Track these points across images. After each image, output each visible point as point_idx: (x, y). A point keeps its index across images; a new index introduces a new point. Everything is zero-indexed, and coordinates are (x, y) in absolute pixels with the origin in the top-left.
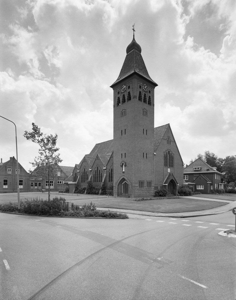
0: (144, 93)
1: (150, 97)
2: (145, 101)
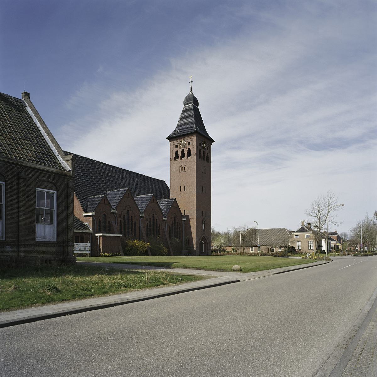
0: (203, 150)
1: (207, 153)
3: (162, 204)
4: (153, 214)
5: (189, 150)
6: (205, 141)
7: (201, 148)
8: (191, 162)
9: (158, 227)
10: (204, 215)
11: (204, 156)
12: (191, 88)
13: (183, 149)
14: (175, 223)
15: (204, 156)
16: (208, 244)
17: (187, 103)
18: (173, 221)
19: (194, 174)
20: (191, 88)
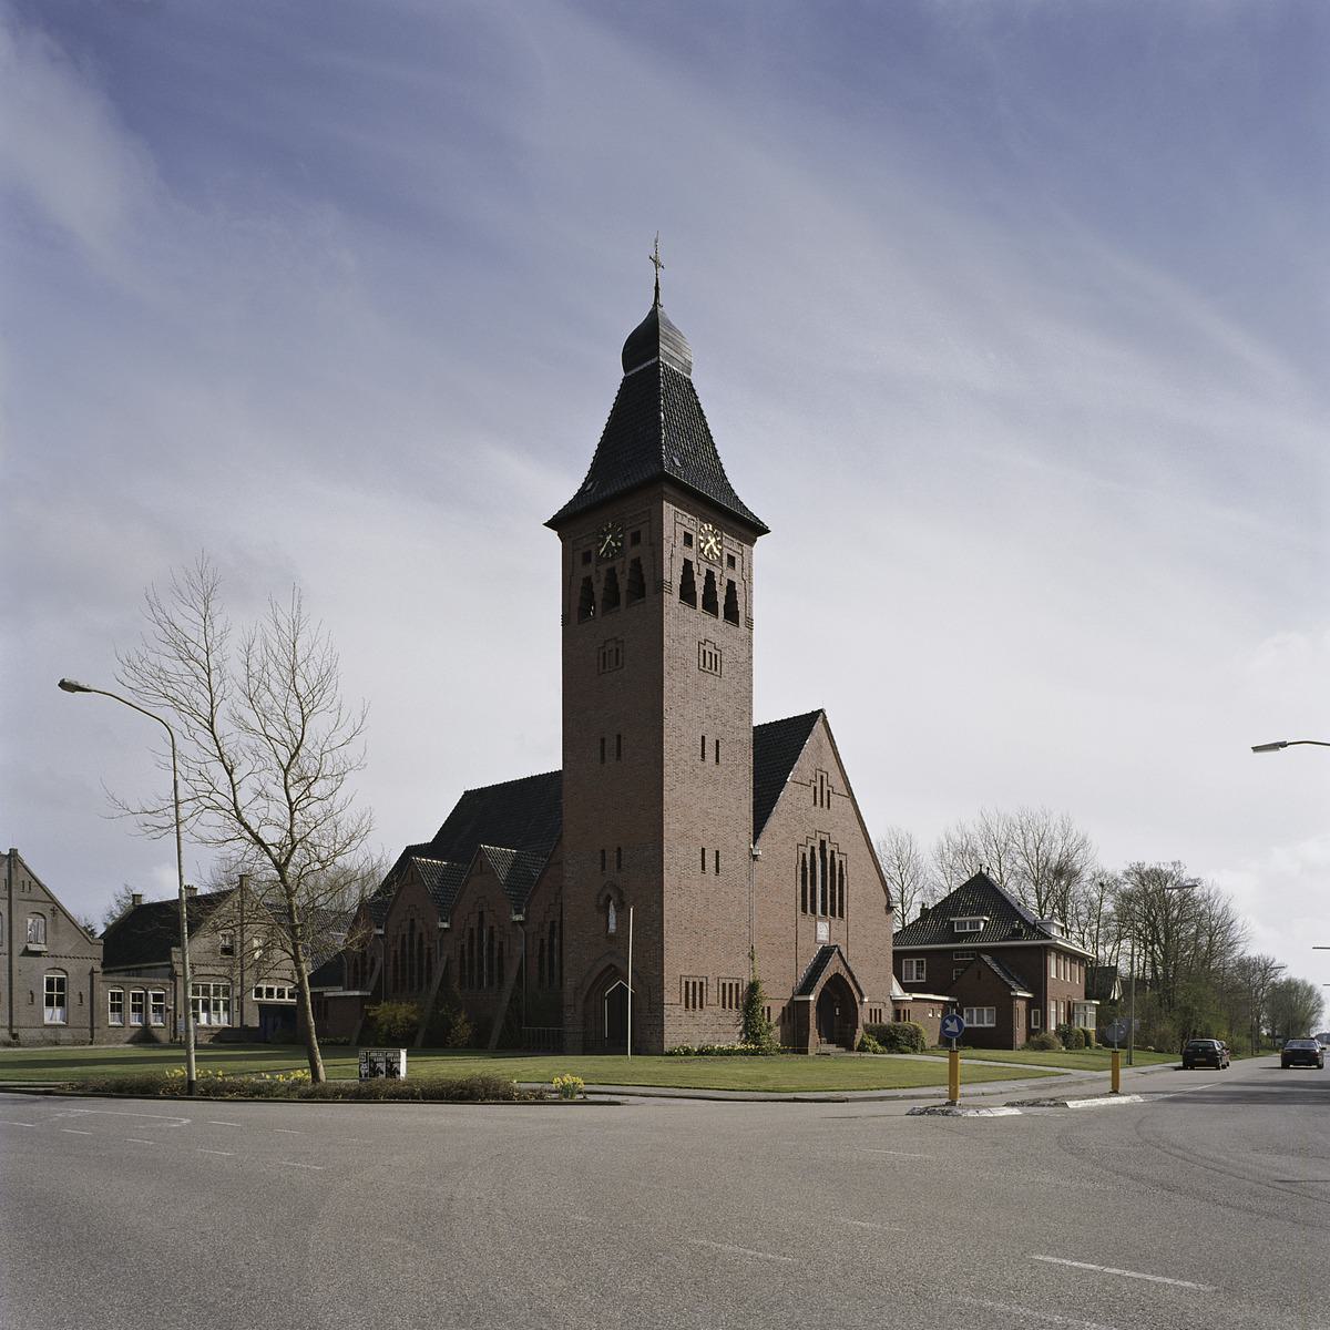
0: (707, 566)
2: (710, 605)
12: (657, 288)
20: (657, 288)
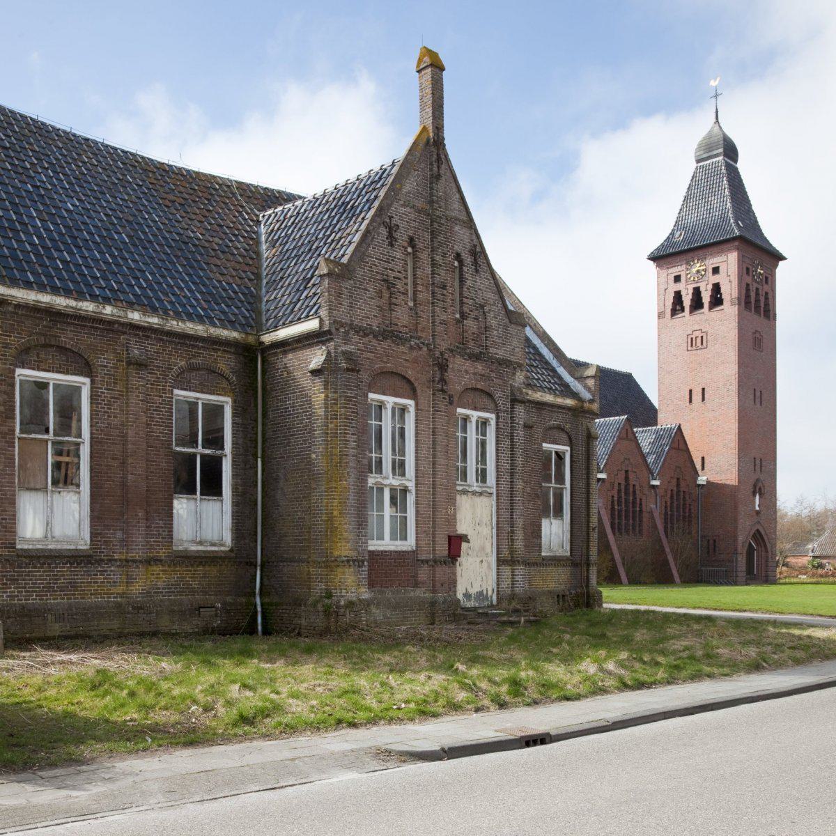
0: (756, 285)
1: (767, 293)
3: (645, 437)
4: (627, 472)
5: (716, 288)
6: (760, 257)
7: (749, 280)
8: (723, 324)
9: (638, 505)
10: (758, 468)
11: (757, 301)
12: (717, 112)
13: (695, 285)
14: (678, 492)
15: (757, 301)
16: (767, 552)
17: (704, 156)
18: (675, 489)
19: (732, 355)
20: (717, 112)
